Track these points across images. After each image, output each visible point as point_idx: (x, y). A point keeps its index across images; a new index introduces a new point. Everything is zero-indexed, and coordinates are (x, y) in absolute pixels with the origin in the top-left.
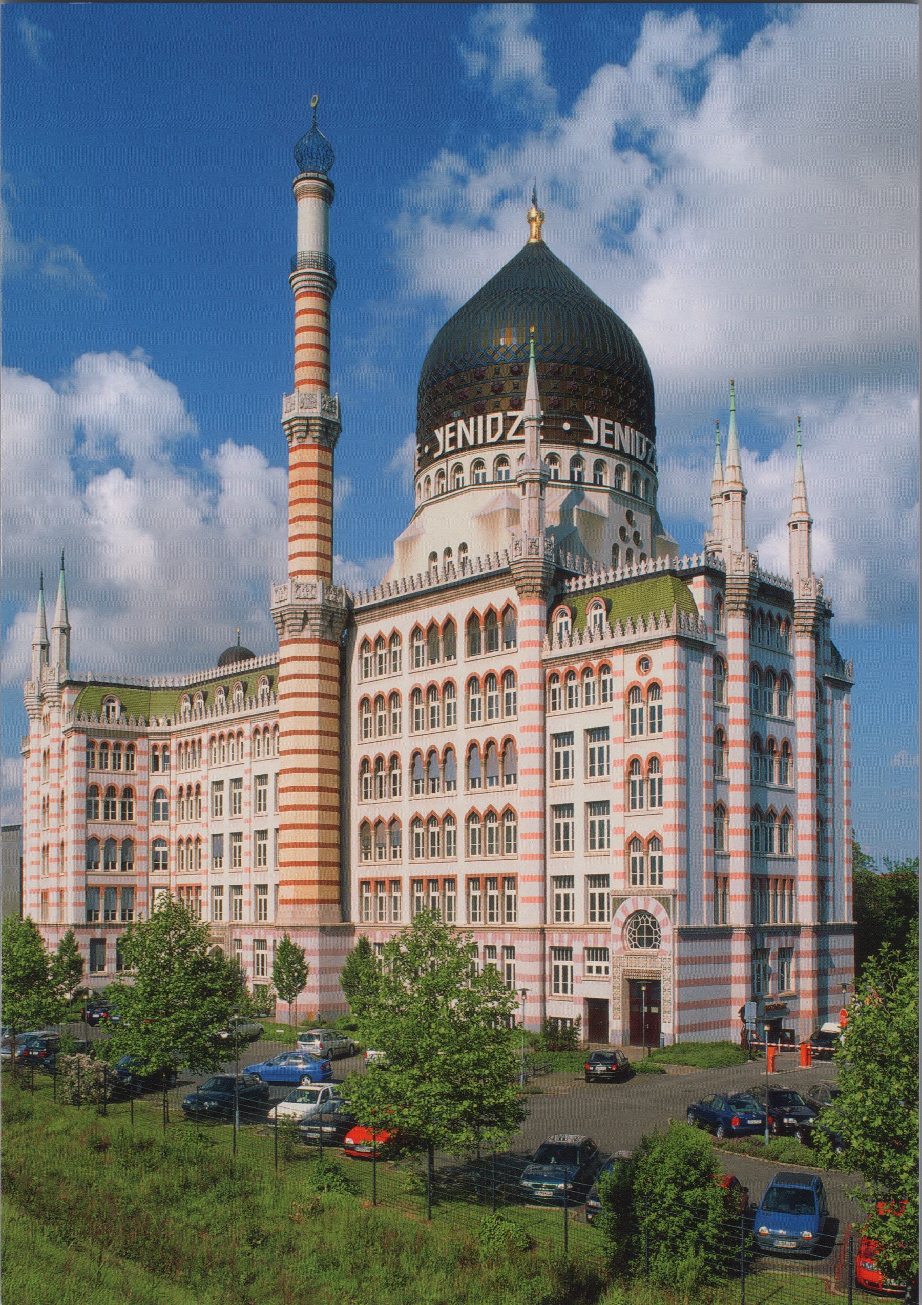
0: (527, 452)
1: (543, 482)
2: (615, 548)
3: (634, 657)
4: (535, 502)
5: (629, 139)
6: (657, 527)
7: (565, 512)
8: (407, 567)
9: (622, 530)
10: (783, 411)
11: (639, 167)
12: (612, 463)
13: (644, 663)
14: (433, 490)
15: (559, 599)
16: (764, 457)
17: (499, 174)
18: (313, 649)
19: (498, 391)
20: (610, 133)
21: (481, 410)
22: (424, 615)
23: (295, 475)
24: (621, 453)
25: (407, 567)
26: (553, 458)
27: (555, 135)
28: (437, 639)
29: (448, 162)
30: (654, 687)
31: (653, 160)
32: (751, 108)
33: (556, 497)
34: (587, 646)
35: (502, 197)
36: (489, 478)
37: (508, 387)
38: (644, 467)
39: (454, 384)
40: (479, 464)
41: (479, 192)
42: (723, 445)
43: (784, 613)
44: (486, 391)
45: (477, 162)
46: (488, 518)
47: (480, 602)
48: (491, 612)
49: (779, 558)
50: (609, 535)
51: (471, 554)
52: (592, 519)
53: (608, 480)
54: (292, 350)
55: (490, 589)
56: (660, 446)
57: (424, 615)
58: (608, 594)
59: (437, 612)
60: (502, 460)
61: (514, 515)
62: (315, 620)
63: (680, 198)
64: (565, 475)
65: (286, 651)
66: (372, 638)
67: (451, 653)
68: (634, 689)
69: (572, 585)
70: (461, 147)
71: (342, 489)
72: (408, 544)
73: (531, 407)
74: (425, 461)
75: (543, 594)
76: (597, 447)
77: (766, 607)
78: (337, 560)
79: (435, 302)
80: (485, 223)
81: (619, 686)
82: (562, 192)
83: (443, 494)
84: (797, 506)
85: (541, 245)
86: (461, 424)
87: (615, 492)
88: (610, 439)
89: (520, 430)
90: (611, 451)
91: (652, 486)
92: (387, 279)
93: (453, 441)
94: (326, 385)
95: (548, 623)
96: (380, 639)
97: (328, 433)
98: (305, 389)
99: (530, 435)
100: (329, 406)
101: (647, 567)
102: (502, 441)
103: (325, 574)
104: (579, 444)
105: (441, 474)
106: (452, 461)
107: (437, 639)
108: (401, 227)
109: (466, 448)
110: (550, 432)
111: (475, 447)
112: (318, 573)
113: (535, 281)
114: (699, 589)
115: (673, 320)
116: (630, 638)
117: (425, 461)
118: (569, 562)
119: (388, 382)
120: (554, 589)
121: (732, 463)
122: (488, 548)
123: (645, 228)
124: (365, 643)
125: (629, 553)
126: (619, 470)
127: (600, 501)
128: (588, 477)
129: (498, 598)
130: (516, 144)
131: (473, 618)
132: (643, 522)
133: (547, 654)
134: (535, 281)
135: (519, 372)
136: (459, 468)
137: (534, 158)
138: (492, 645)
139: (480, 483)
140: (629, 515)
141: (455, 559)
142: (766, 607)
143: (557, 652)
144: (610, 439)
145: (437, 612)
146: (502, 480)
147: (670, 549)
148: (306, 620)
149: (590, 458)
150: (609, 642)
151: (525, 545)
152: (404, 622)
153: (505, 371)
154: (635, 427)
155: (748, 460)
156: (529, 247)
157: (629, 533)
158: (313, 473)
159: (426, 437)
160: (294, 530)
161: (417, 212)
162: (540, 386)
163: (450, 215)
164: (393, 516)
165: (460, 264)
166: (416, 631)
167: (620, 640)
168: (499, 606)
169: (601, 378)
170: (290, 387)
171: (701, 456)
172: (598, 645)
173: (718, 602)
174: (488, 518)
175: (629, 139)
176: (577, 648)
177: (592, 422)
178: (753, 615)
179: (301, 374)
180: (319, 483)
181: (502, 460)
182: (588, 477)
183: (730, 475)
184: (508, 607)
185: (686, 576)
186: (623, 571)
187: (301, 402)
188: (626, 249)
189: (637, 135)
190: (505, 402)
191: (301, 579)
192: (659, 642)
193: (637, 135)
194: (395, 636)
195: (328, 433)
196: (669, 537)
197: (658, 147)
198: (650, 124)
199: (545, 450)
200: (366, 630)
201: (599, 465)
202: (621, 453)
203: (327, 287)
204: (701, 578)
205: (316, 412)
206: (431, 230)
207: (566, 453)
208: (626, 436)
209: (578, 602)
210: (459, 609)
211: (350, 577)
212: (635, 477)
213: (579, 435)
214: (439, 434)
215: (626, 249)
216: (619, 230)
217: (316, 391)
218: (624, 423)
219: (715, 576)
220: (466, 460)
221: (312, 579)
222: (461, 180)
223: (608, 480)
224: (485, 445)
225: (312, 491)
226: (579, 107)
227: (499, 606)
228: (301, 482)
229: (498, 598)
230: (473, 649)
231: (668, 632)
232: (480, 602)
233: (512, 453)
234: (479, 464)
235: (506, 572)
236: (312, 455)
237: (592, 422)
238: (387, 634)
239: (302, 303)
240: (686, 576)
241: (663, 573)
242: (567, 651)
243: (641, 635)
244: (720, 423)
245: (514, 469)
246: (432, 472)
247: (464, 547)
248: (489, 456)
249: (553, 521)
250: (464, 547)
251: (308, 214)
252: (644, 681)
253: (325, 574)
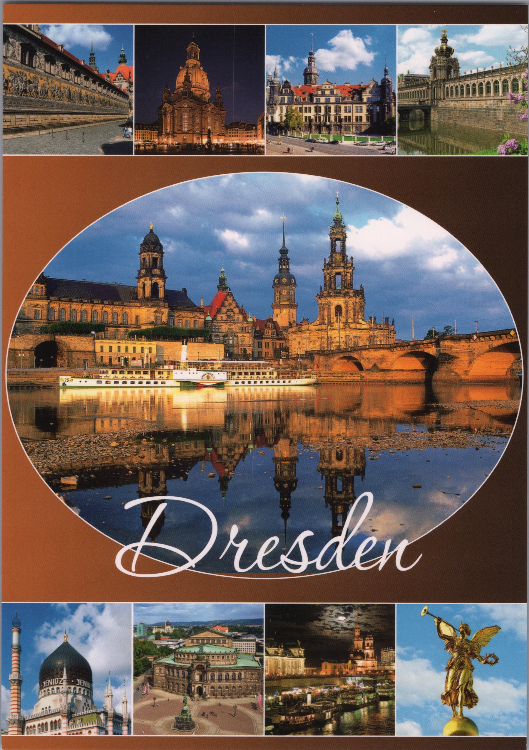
0: (64, 687)
1: (68, 693)
2: (83, 707)
3: (87, 731)
4: (65, 698)
5: (87, 620)
6: (93, 703)
7: (72, 700)
8: (37, 711)
9: (85, 703)
10: (121, 678)
11: (89, 626)
12: (83, 689)
14: (43, 695)
15: (71, 718)
16: (116, 688)
17: (58, 627)
18: (16, 729)
19: (57, 673)
20: (82, 618)
21: (53, 678)
22: (41, 722)
23: (12, 691)
24: (85, 687)
25: (37, 711)
26: (70, 688)
27: (70, 618)
28: (43, 727)
29: (46, 624)
31: (92, 624)
32: (114, 613)
33: (70, 696)
34: (77, 728)
35: (58, 632)
36: (55, 692)
37: (59, 673)
38: (90, 690)
39: (48, 672)
40: (53, 689)
41: (53, 631)
42: (108, 685)
43: (121, 721)
44: (55, 673)
45: (53, 625)
46: (55, 701)
47: (53, 719)
48: (56, 721)
49: (120, 709)
50: (82, 704)
51: (52, 709)
52: (78, 701)
53: (82, 692)
54: (11, 661)
55: (55, 716)
56: (93, 685)
57: (41, 722)
58: (82, 717)
59: (44, 721)
60: (58, 688)
61: (61, 700)
62: (16, 722)
63: (98, 632)
64: (72, 691)
65: (10, 729)
66: (29, 726)
67: (47, 730)
69: (74, 715)
70: (49, 621)
71: (23, 694)
72: (37, 706)
73: (65, 677)
74: (41, 688)
75: (67, 717)
76: (79, 686)
77: (117, 720)
78: (21, 710)
79: (44, 654)
80: (55, 638)
82: (72, 631)
83: (45, 696)
84: (124, 698)
85: (67, 642)
86: (49, 681)
87: (83, 695)
88: (82, 684)
89: (62, 682)
90: (82, 686)
91: (92, 694)
92: (33, 650)
93: (47, 684)
94: (19, 672)
95: (68, 723)
96: (31, 727)
97: (19, 682)
98: (14, 673)
99: (64, 683)
100: (20, 676)
101: (91, 711)
102: (58, 684)
103: (19, 713)
104: (76, 685)
105: (45, 691)
106: (47, 688)
107: (43, 727)
108: (36, 638)
109: (50, 686)
110: (69, 682)
111: (52, 685)
112: (17, 712)
113: (66, 650)
114: (102, 716)
115: (96, 658)
117: (41, 688)
118: (73, 710)
119: (33, 672)
120: (70, 716)
121: (109, 689)
123: (90, 639)
124: (28, 727)
125: (86, 709)
126: (84, 691)
127: (80, 697)
128: (77, 692)
129: (57, 718)
130: (61, 620)
131: (52, 722)
132: (90, 702)
133: (68, 730)
134: (66, 650)
135: (62, 670)
136: (48, 690)
137: (66, 624)
138: (56, 728)
139: (53, 693)
140: (86, 700)
141: (48, 710)
142: (117, 720)
143: (71, 730)
144: (82, 684)
145: (44, 721)
146: (58, 693)
147: (95, 707)
148: (14, 722)
149: (78, 688)
150: (82, 727)
151: (63, 707)
152: (36, 723)
153: (59, 669)
154: (88, 681)
155: (113, 688)
156: (64, 643)
157: (87, 704)
158: (16, 691)
159: (41, 683)
160: (12, 703)
161: (39, 635)
162: (67, 673)
163: (47, 636)
164: (33, 700)
165: (49, 646)
166: (39, 725)
167: (84, 727)
168: (57, 720)
169: (80, 671)
170: (11, 673)
171: (102, 688)
172: (80, 728)
173: (106, 719)
174: (55, 701)
175: (87, 620)
176: (75, 729)
177: (78, 680)
178: (114, 722)
179: (13, 670)
180: (18, 693)
181: (58, 688)
182: (77, 692)
183: (109, 692)
184: (59, 720)
185: (99, 714)
186: (85, 712)
187: (13, 676)
188: (86, 643)
189: (88, 619)
190: (59, 676)
191: (13, 714)
192: (93, 727)
193: (88, 619)
194: (34, 726)
195: (19, 682)
196: (95, 705)
197: (93, 621)
198: (91, 616)
199: (68, 686)
200: (28, 725)
201: (80, 689)
202: (85, 687)
203: (19, 650)
204: (102, 714)
205: (17, 678)
206: (43, 639)
207: (72, 687)
208: (85, 683)
209: (75, 719)
210: (49, 720)
211: (25, 714)
212: (88, 692)
213: (75, 684)
214: (44, 683)
215: (86, 643)
216: (84, 640)
217: (17, 674)
218: (85, 681)
219: (106, 713)
220: (50, 688)
221: (16, 714)
222: (49, 628)
223: (82, 692)
224: (54, 685)
225: (16, 695)
226: (76, 613)
227: (57, 720)
228: (14, 693)
229: (57, 718)
230: (52, 729)
231: (94, 725)
232: (53, 719)
233: (61, 687)
234: (53, 689)
235: (59, 712)
236: (16, 687)
237: (78, 680)
238: (32, 725)
239: (14, 655)
240: (99, 714)
241: (94, 713)
242: (73, 729)
243: (89, 726)
244: (107, 681)
245: (61, 690)
246: (43, 691)
247: (50, 707)
248: (55, 687)
249: (69, 701)
250: (50, 707)
251: (15, 636)
253: (19, 713)
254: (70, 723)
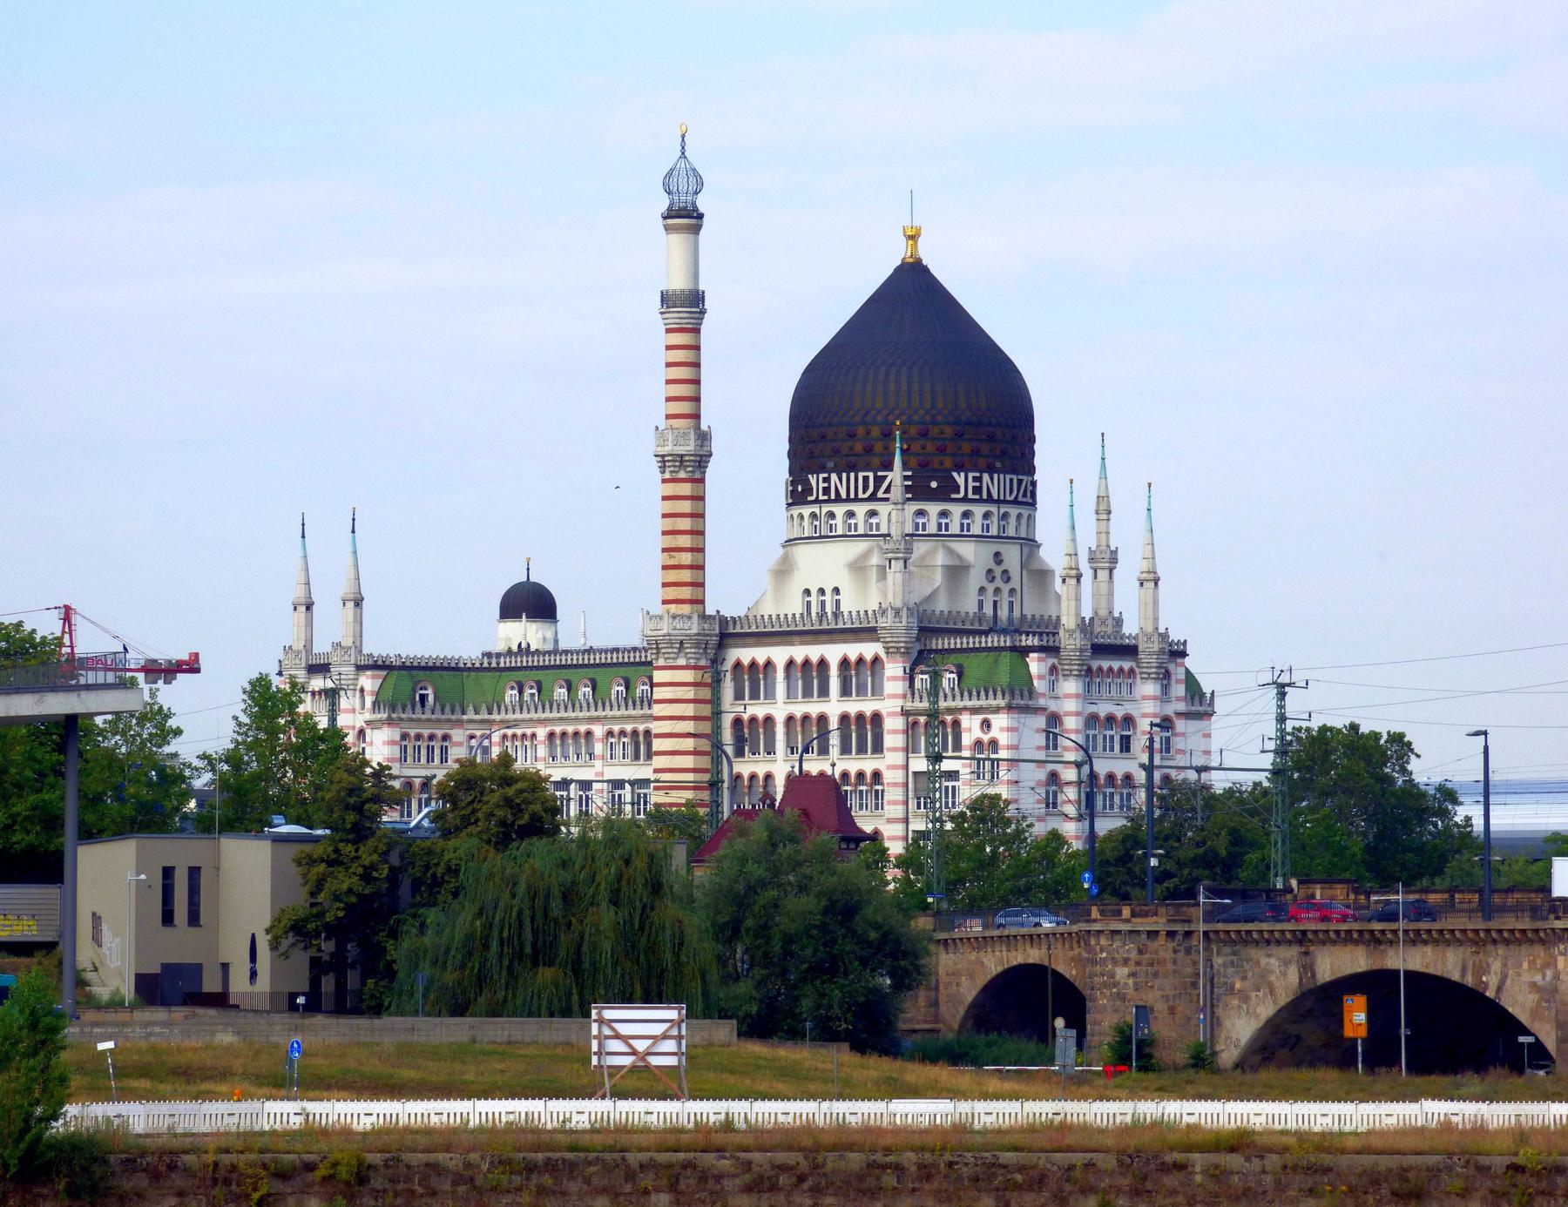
3: (978, 718)
13: (986, 725)
21: (853, 468)
22: (799, 652)
30: (994, 744)
37: (878, 447)
44: (859, 448)
57: (799, 652)
59: (814, 652)
68: (978, 744)
81: (967, 740)
88: (977, 490)
89: (888, 490)
93: (826, 491)
102: (873, 498)
106: (826, 508)
107: (811, 676)
109: (838, 499)
111: (848, 500)
116: (974, 703)
129: (869, 650)
133: (909, 705)
145: (814, 652)
149: (956, 510)
150: (959, 703)
152: (779, 655)
184: (876, 659)
207: (933, 509)
210: (833, 653)
213: (946, 492)
214: (813, 480)
218: (991, 470)
220: (840, 510)
224: (857, 500)
229: (869, 650)
232: (853, 650)
248: (861, 510)
252: (986, 738)
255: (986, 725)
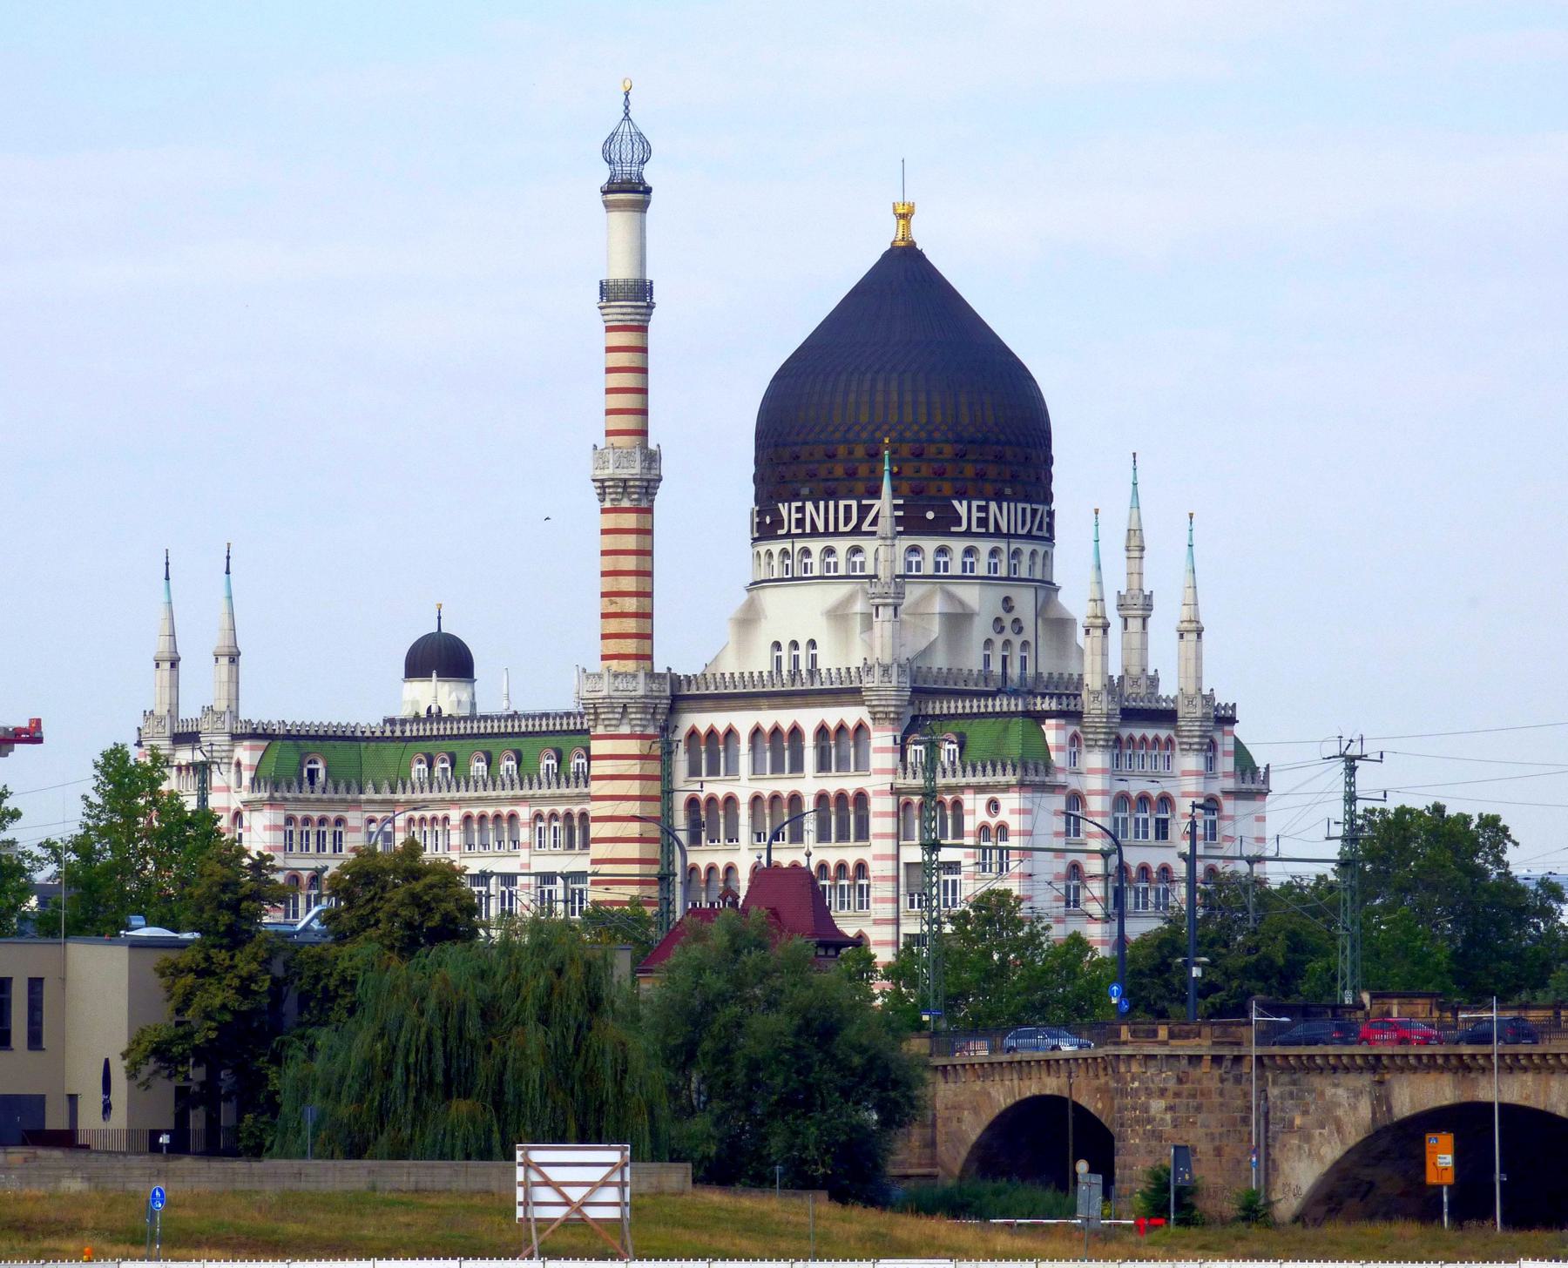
3: (983, 799)
13: (994, 806)
22: (768, 718)
30: (1003, 829)
37: (863, 470)
44: (839, 471)
57: (768, 718)
59: (785, 718)
68: (984, 828)
81: (970, 824)
88: (983, 522)
89: (874, 522)
93: (800, 523)
102: (857, 531)
106: (800, 544)
107: (781, 748)
109: (815, 533)
111: (826, 534)
116: (980, 779)
122: (837, 657)
133: (900, 782)
145: (785, 718)
153: (860, 451)
177: (961, 508)
184: (860, 727)
207: (930, 544)
210: (809, 719)
218: (999, 498)
220: (816, 546)
224: (837, 533)
232: (833, 716)
233: (869, 545)
248: (842, 545)
252: (993, 822)
254: (912, 750)
255: (994, 806)
